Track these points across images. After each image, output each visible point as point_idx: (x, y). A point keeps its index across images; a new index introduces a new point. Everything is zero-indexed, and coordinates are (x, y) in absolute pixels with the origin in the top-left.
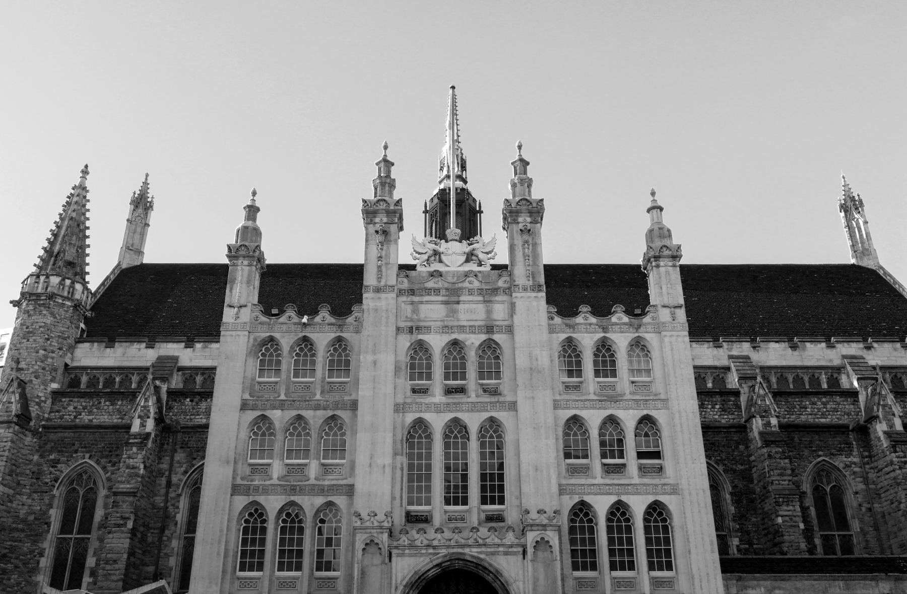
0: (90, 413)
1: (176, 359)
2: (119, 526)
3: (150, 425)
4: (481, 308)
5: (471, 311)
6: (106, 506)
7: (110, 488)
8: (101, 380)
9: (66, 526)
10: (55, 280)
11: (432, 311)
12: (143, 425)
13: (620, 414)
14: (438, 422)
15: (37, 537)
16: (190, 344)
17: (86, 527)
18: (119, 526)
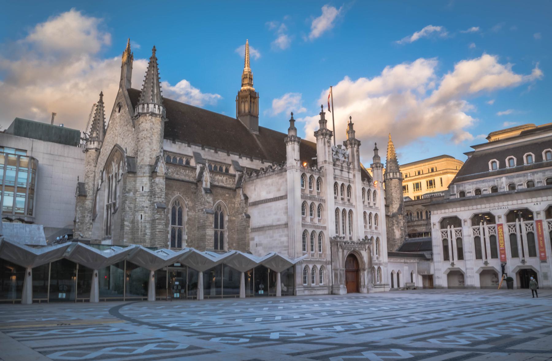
0: (177, 174)
1: (199, 154)
2: (210, 226)
3: (209, 186)
4: (347, 173)
5: (345, 174)
6: (188, 215)
7: (189, 208)
8: (172, 158)
9: (174, 222)
10: (161, 108)
11: (338, 172)
12: (206, 185)
13: (372, 212)
14: (341, 208)
15: (167, 225)
16: (203, 149)
17: (180, 223)
18: (210, 226)
